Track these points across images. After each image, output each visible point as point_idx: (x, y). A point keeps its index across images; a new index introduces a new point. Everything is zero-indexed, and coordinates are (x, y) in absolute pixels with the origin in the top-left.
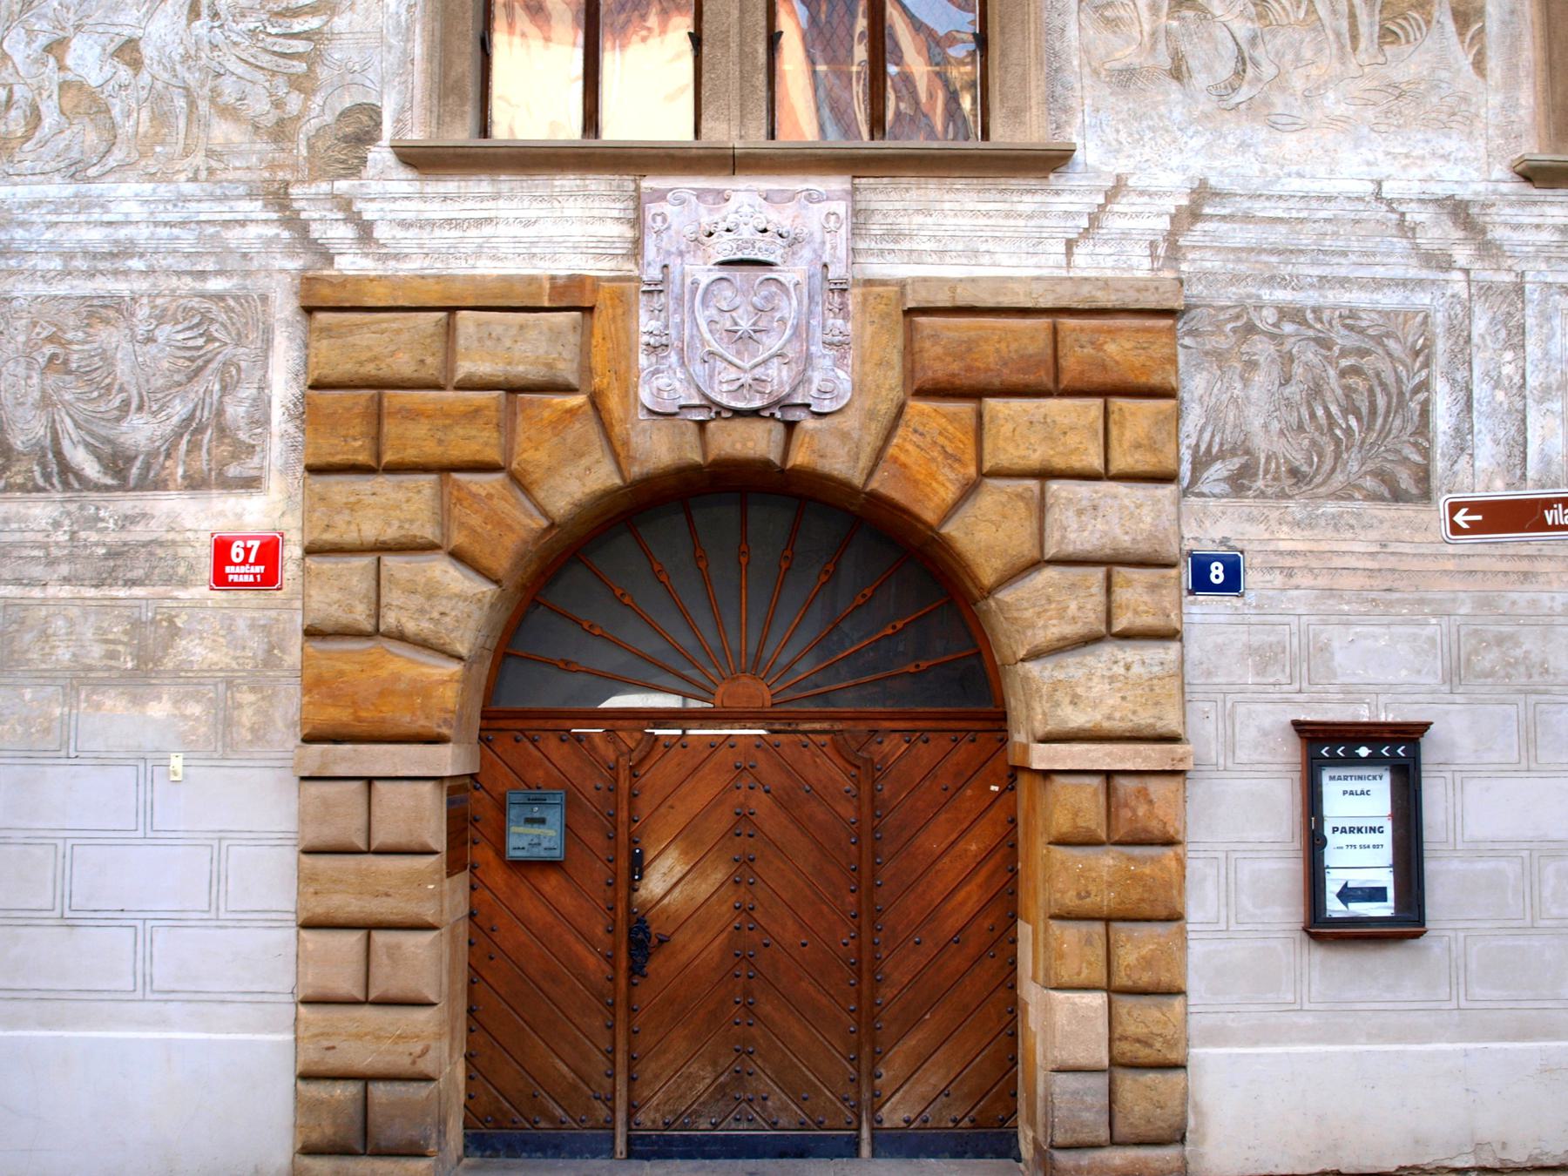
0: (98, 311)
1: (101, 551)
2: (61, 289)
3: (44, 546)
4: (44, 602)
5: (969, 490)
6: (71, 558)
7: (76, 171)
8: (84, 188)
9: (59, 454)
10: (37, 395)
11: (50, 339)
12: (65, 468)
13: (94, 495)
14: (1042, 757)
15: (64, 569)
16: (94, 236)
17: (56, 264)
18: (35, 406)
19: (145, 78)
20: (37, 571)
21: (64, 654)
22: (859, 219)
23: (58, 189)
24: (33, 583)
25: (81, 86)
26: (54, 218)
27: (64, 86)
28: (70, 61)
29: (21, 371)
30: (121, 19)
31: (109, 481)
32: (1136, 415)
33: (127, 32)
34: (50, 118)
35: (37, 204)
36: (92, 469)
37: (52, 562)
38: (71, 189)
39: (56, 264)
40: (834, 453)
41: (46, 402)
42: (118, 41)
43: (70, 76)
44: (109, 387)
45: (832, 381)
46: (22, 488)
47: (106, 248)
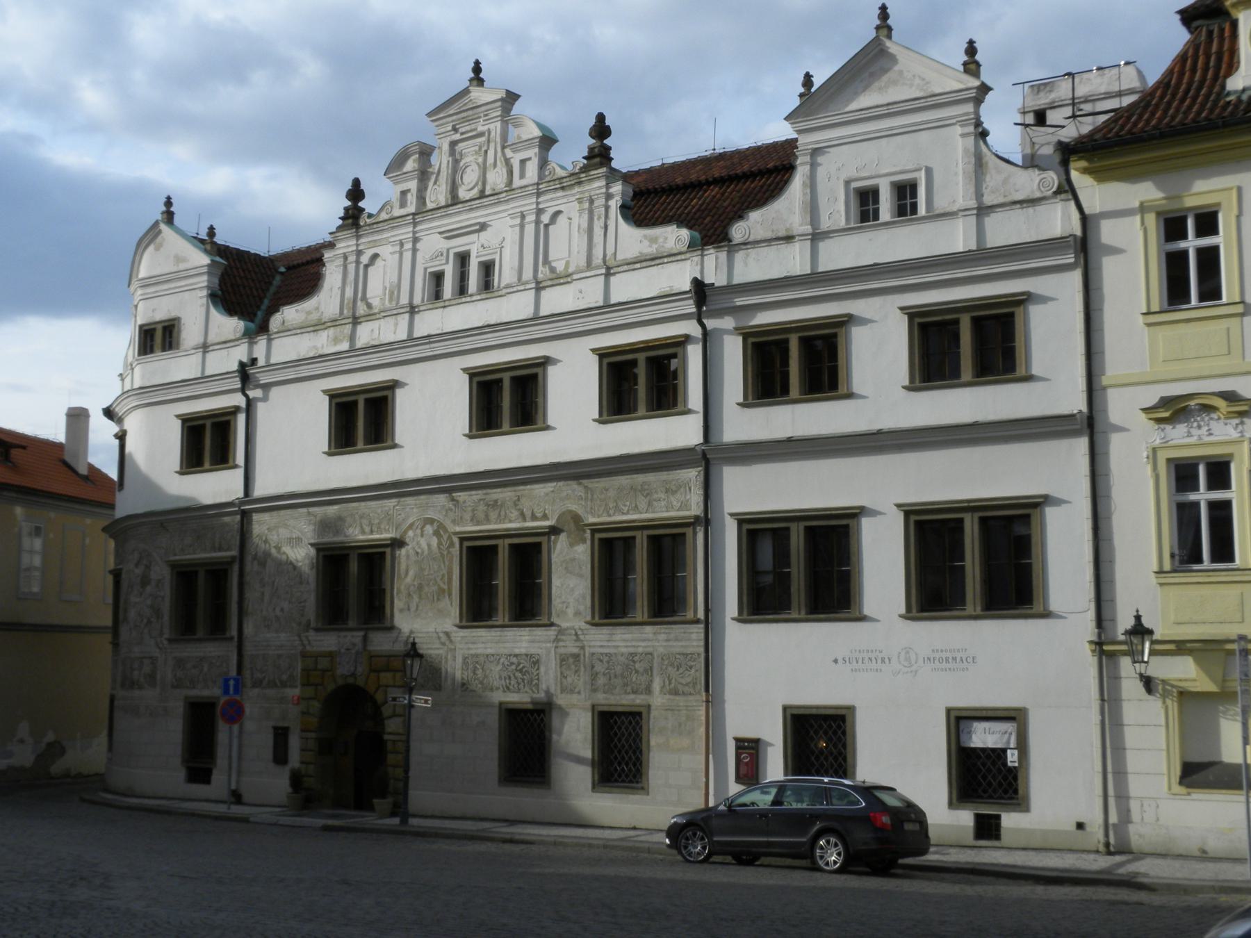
0: (279, 656)
5: (377, 689)
14: (386, 737)
22: (365, 639)
32: (399, 675)
40: (360, 682)
45: (360, 670)
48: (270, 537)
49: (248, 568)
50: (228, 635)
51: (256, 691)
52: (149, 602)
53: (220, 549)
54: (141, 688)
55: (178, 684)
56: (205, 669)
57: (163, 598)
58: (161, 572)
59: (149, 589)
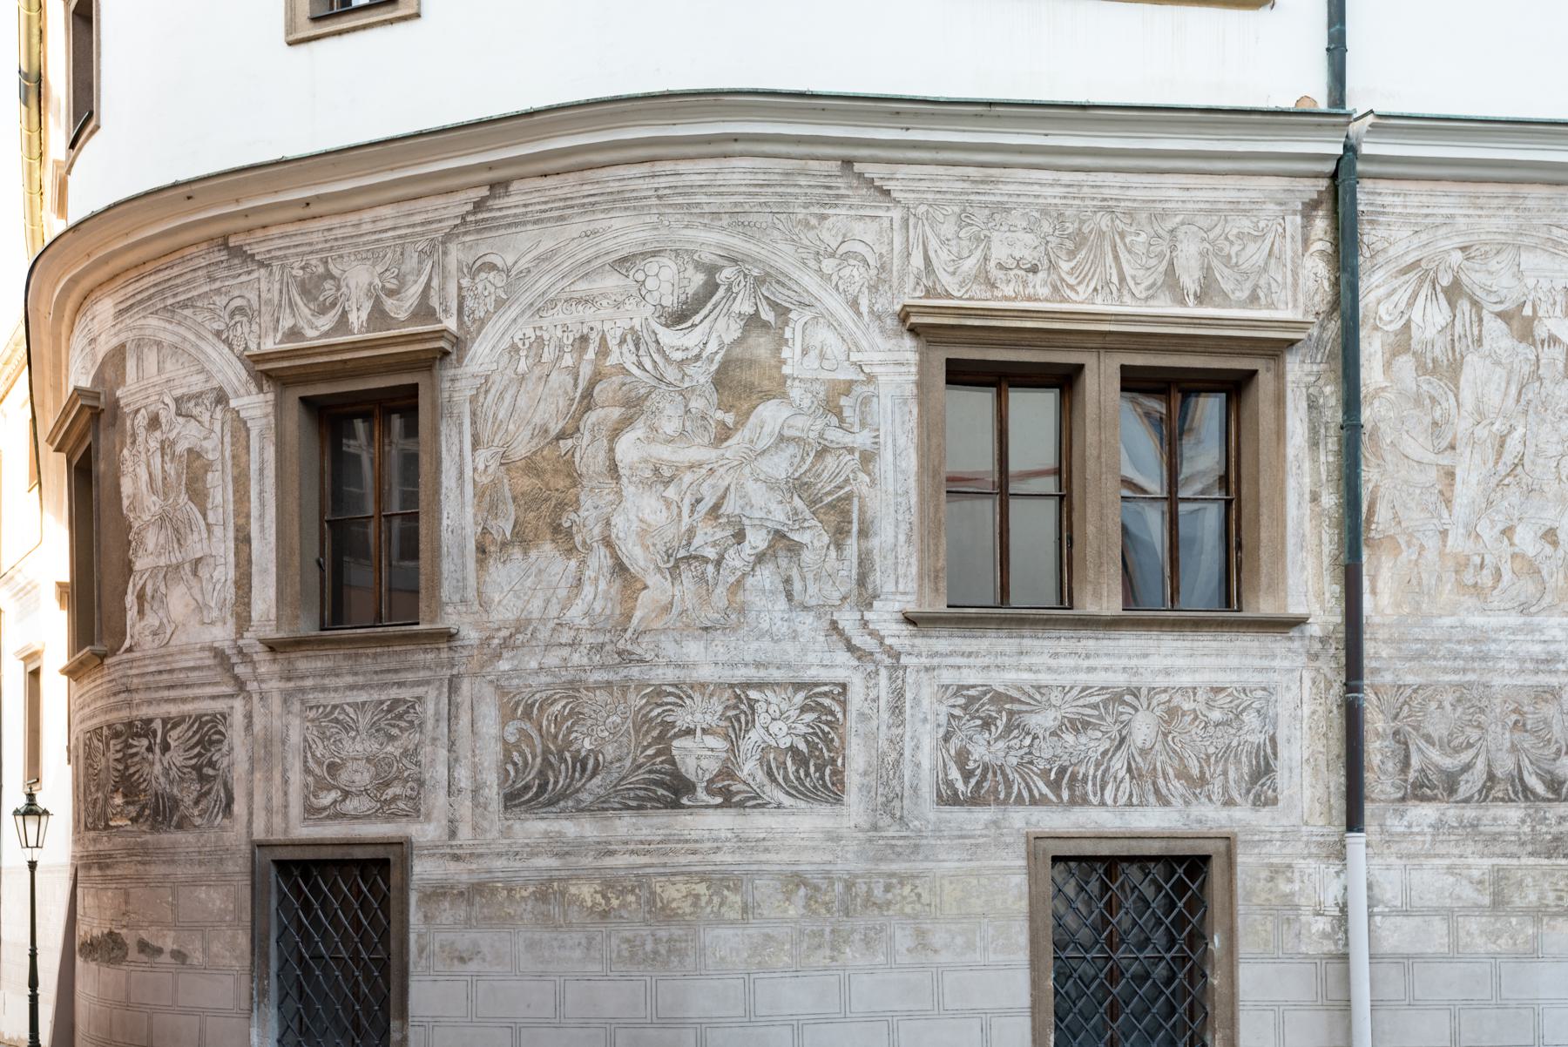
1: (1549, 837)
2: (1519, 681)
3: (1517, 834)
4: (1519, 867)
6: (1533, 842)
7: (1523, 609)
8: (1529, 619)
9: (1521, 779)
10: (1508, 745)
11: (1514, 711)
12: (1525, 788)
13: (1543, 804)
15: (1530, 848)
16: (1537, 649)
17: (1516, 666)
18: (1509, 751)
19: (1561, 553)
20: (1514, 849)
21: (1533, 897)
23: (1514, 620)
24: (1512, 856)
25: (1523, 556)
26: (1512, 637)
27: (1514, 556)
28: (1516, 540)
29: (1499, 729)
30: (1544, 515)
31: (1550, 796)
33: (1549, 524)
34: (1507, 576)
35: (1503, 629)
36: (1540, 789)
37: (1523, 844)
38: (1521, 620)
39: (1516, 666)
41: (1514, 749)
42: (1544, 529)
43: (1517, 550)
44: (1549, 741)
46: (1502, 800)
47: (1543, 656)
48: (1474, 278)
49: (1372, 374)
50: (1265, 607)
51: (1424, 813)
52: (779, 466)
53: (1200, 300)
54: (729, 800)
55: (976, 788)
56: (1143, 729)
57: (867, 458)
58: (852, 354)
59: (770, 415)
